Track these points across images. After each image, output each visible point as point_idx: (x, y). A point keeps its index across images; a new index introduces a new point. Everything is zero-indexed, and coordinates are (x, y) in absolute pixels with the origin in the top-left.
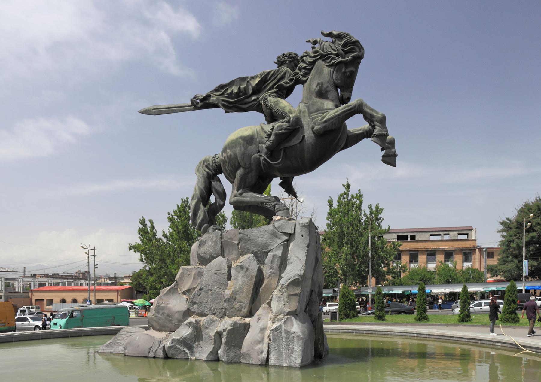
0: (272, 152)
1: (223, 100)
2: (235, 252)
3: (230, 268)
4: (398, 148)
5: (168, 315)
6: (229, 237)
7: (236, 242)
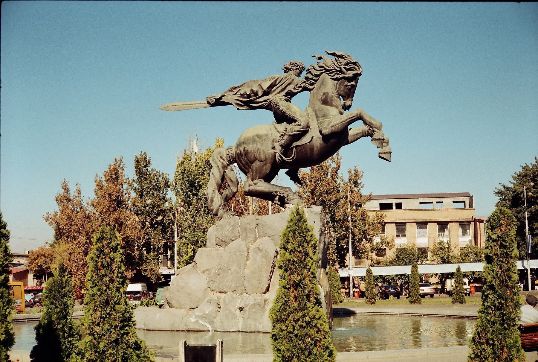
0: (286, 149)
2: (253, 236)
3: (248, 249)
4: (391, 147)
5: (189, 294)
6: (247, 222)
7: (254, 227)
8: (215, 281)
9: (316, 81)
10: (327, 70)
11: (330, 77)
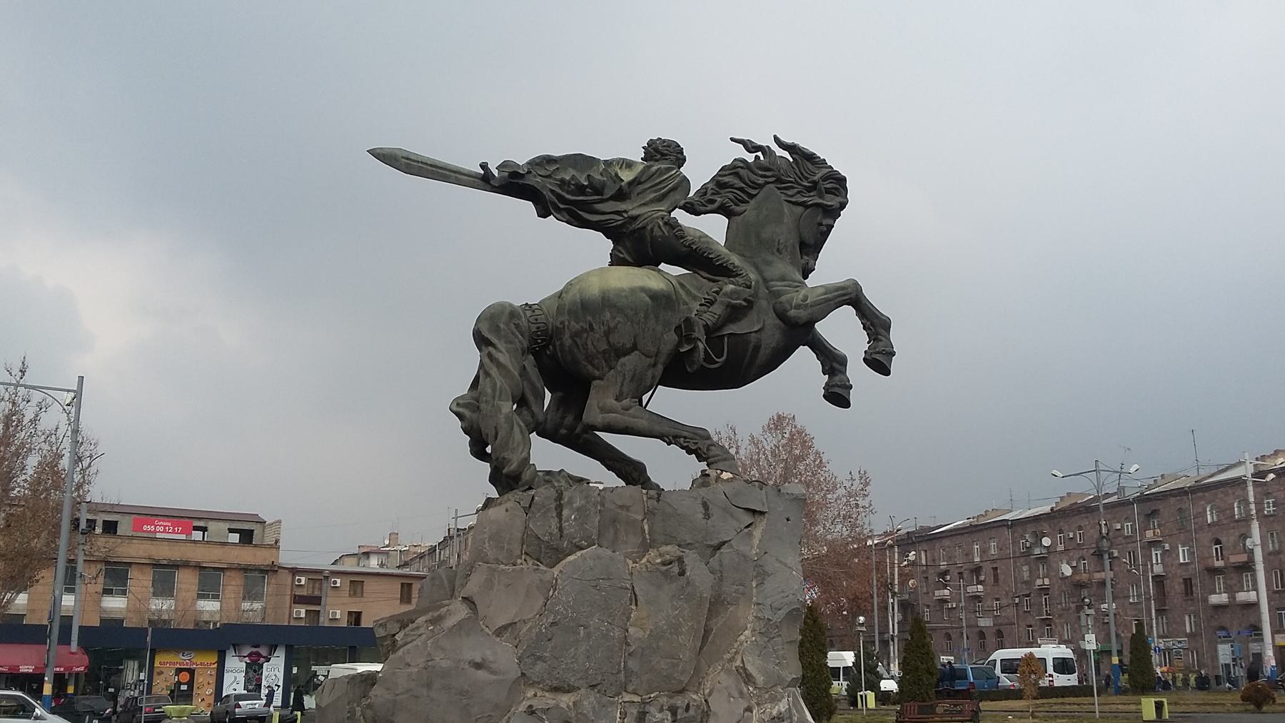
1: (552, 191)
5: (462, 693)
7: (640, 517)
8: (540, 658)
9: (752, 196)
10: (779, 180)
11: (783, 197)
